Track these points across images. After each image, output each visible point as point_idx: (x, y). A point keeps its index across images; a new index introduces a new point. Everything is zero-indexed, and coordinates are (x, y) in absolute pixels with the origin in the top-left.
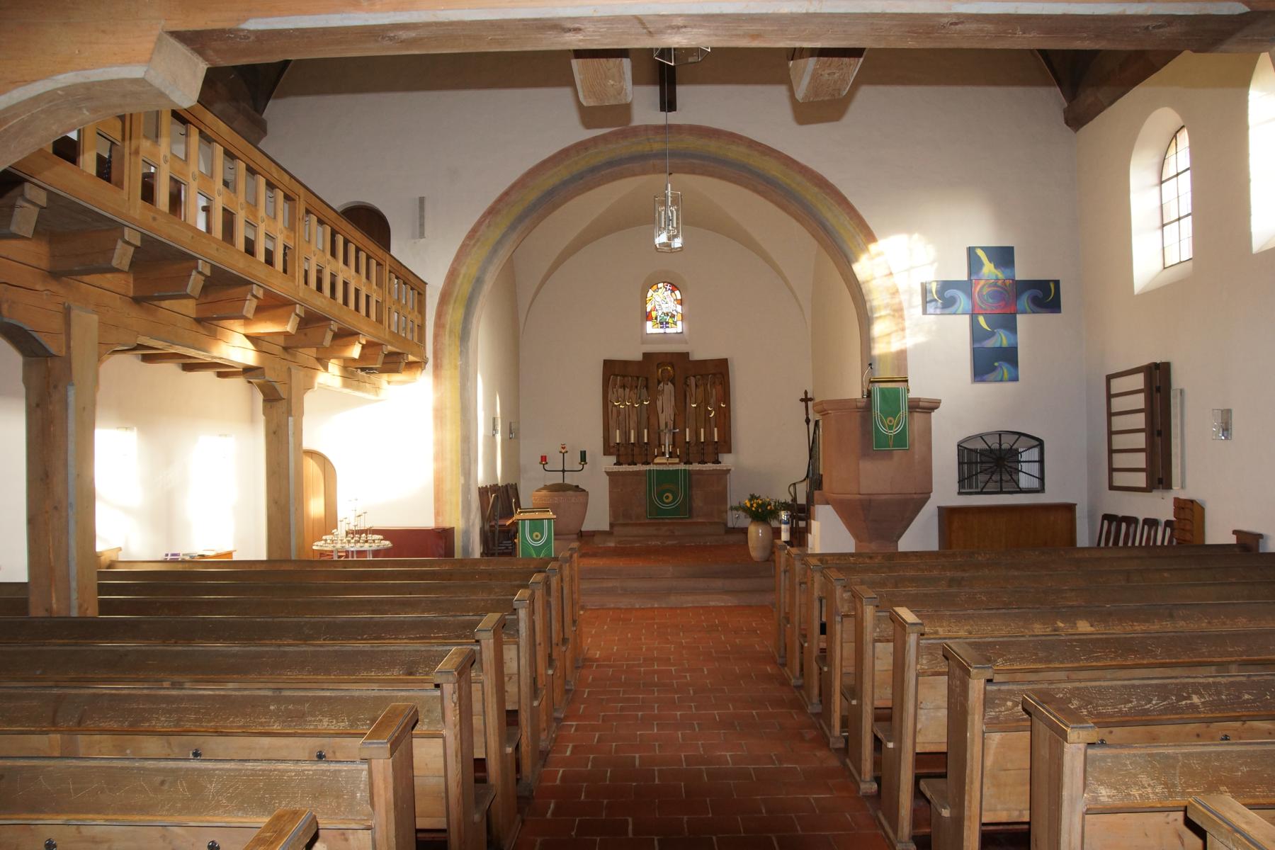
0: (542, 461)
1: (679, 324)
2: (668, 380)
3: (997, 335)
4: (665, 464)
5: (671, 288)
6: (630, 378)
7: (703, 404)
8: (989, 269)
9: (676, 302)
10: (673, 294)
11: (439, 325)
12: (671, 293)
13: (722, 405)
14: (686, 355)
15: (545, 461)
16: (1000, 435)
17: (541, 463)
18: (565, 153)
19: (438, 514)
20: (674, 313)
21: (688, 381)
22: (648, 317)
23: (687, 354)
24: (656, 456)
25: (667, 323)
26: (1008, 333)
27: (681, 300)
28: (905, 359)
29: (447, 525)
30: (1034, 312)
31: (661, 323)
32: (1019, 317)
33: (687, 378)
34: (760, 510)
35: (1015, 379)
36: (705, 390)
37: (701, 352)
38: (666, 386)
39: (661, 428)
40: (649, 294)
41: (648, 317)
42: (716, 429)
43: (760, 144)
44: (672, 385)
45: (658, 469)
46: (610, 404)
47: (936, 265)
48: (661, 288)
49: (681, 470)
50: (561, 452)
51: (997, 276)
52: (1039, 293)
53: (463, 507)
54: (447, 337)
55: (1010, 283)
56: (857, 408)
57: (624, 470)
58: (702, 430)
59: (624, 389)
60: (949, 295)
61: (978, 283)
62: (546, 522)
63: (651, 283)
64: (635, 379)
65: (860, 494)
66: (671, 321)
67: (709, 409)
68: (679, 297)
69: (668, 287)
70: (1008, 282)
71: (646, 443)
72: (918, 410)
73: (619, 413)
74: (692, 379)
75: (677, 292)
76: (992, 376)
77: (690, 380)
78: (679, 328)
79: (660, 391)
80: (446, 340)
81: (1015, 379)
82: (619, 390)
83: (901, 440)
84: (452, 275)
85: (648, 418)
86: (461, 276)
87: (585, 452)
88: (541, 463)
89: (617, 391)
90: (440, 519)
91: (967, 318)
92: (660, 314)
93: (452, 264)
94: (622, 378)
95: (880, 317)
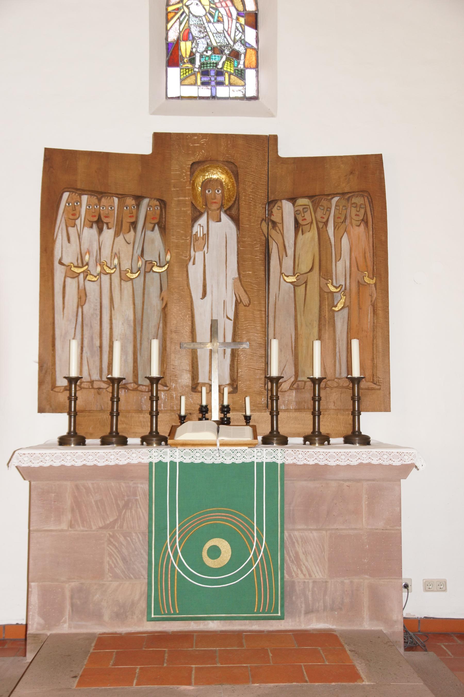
6: (116, 200)
7: (315, 276)
20: (239, 47)
21: (275, 210)
24: (183, 419)
25: (220, 73)
31: (205, 73)
38: (213, 224)
39: (199, 339)
42: (355, 344)
45: (187, 460)
46: (59, 272)
49: (260, 465)
58: (317, 345)
59: (100, 231)
64: (130, 202)
66: (229, 68)
67: (333, 289)
71: (154, 381)
74: (287, 206)
77: (281, 208)
79: (197, 239)
82: (86, 230)
85: (164, 309)
92: (202, 46)
94: (94, 200)
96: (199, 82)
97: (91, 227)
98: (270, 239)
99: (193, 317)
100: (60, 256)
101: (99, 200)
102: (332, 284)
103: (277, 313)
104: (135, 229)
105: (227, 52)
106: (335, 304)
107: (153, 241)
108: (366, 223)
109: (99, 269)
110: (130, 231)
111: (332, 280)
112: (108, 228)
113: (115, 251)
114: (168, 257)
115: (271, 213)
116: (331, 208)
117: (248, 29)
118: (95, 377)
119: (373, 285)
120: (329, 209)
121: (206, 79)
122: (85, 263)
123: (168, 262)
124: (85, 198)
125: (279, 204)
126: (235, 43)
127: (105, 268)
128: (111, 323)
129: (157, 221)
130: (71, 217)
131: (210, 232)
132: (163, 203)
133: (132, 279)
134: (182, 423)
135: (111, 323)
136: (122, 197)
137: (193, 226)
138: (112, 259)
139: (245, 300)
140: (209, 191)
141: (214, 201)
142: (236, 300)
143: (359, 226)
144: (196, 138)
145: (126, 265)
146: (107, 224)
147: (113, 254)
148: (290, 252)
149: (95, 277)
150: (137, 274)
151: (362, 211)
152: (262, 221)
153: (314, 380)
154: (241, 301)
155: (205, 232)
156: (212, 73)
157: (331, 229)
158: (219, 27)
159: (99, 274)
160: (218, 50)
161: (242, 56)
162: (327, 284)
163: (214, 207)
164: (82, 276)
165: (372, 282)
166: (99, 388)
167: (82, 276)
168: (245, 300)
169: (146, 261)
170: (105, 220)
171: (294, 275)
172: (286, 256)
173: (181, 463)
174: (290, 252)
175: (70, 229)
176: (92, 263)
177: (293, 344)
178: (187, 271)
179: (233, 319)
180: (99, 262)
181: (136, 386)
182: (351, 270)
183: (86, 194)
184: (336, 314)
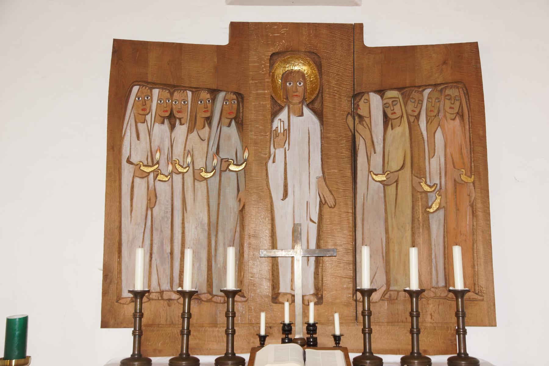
2: (302, 102)
6: (190, 94)
13: (464, 177)
21: (361, 103)
23: (358, 28)
33: (357, 96)
36: (413, 127)
38: (294, 119)
42: (457, 251)
46: (127, 171)
58: (414, 253)
59: (172, 127)
64: (205, 95)
74: (375, 100)
77: (368, 101)
79: (277, 136)
82: (157, 126)
85: (242, 211)
87: (24, 321)
94: (166, 94)
97: (163, 123)
98: (356, 134)
99: (273, 219)
100: (129, 154)
101: (172, 94)
102: (426, 183)
103: (366, 215)
104: (210, 125)
106: (430, 204)
107: (229, 137)
108: (462, 117)
109: (170, 168)
110: (204, 127)
111: (425, 178)
112: (181, 124)
113: (187, 148)
114: (246, 155)
115: (357, 107)
116: (422, 101)
118: (165, 286)
119: (472, 184)
120: (421, 101)
122: (155, 162)
123: (245, 160)
124: (156, 92)
125: (366, 96)
127: (177, 166)
128: (183, 227)
129: (233, 116)
130: (142, 112)
131: (291, 127)
132: (240, 97)
133: (206, 179)
134: (262, 345)
135: (183, 227)
136: (196, 90)
137: (272, 121)
138: (185, 157)
139: (330, 200)
140: (290, 84)
141: (296, 94)
142: (321, 201)
143: (454, 119)
144: (276, 27)
145: (200, 163)
146: (180, 119)
147: (186, 152)
148: (379, 148)
149: (167, 176)
150: (212, 174)
151: (458, 103)
152: (348, 115)
153: (411, 293)
154: (326, 202)
155: (286, 127)
157: (423, 123)
159: (171, 174)
162: (420, 183)
163: (296, 100)
164: (152, 176)
165: (471, 180)
166: (170, 300)
167: (152, 176)
168: (330, 200)
169: (222, 159)
170: (178, 115)
171: (384, 173)
172: (375, 153)
174: (379, 148)
175: (140, 125)
176: (163, 162)
177: (384, 249)
178: (267, 170)
179: (317, 222)
180: (170, 160)
181: (211, 297)
182: (446, 168)
183: (157, 88)
184: (431, 216)
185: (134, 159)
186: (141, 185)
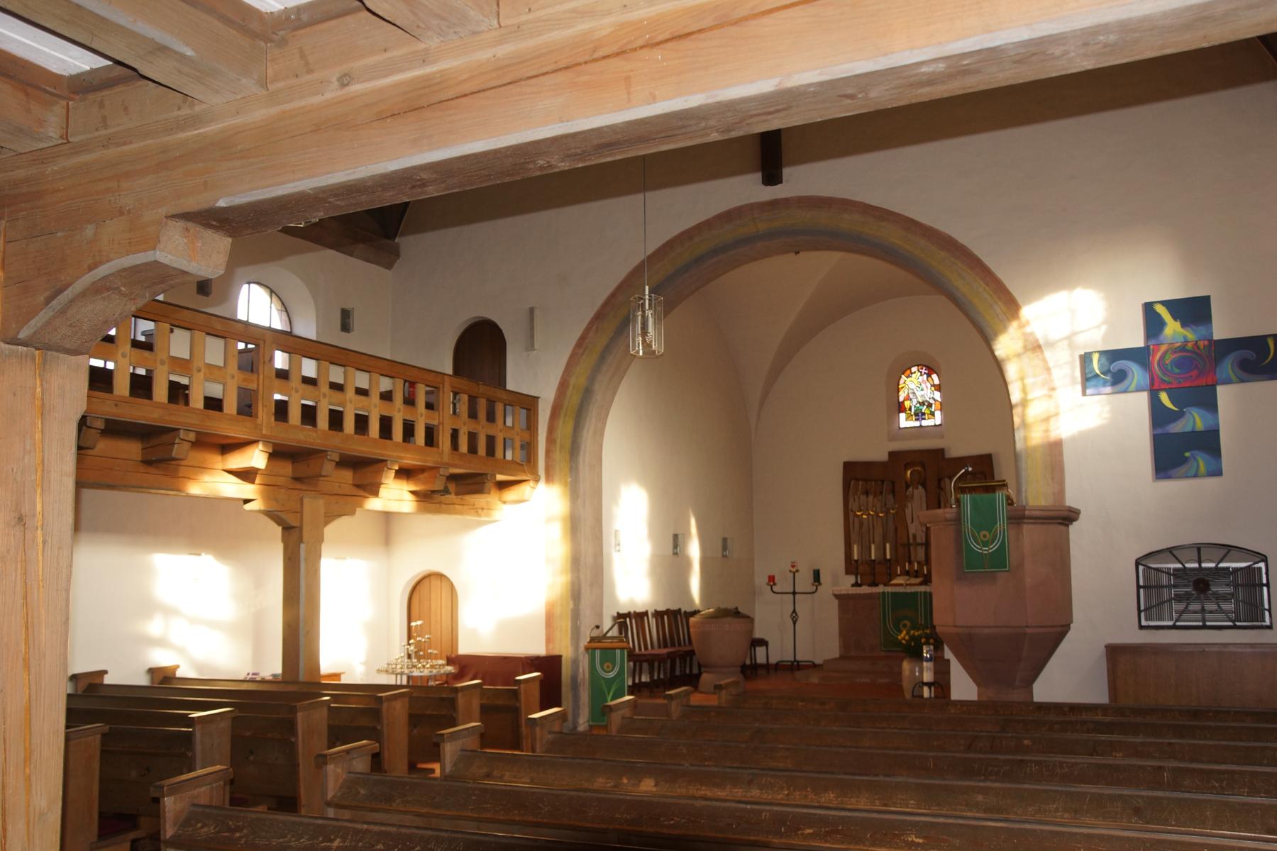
0: (769, 581)
1: (938, 414)
3: (1188, 415)
4: (902, 585)
5: (926, 372)
6: (873, 483)
8: (1173, 329)
9: (933, 389)
10: (930, 379)
11: (550, 440)
12: (927, 377)
14: (941, 452)
15: (774, 581)
16: (1199, 549)
17: (768, 584)
18: (669, 246)
19: (549, 640)
20: (932, 401)
22: (901, 408)
25: (924, 414)
26: (1203, 412)
27: (939, 385)
28: (1061, 454)
29: (556, 652)
30: (1242, 381)
31: (916, 414)
32: (1220, 389)
33: (940, 480)
34: (913, 644)
35: (1218, 472)
37: (958, 448)
38: (915, 491)
40: (902, 381)
41: (901, 408)
43: (876, 208)
44: (923, 491)
46: (851, 513)
47: (1104, 328)
48: (915, 373)
49: (921, 592)
50: (790, 571)
51: (1185, 337)
52: (1250, 354)
53: (572, 634)
54: (558, 452)
55: (1204, 346)
56: (947, 520)
57: (862, 592)
59: (867, 496)
60: (1116, 369)
61: (1158, 350)
62: (618, 652)
63: (906, 370)
64: (879, 483)
65: (955, 626)
68: (937, 382)
69: (923, 371)
70: (1201, 344)
72: (1026, 521)
73: (861, 524)
75: (935, 376)
76: (1182, 470)
78: (938, 419)
80: (557, 455)
81: (1218, 472)
83: (998, 559)
84: (563, 386)
85: (896, 529)
86: (571, 388)
88: (768, 584)
89: (859, 498)
90: (551, 646)
91: (1142, 399)
92: (915, 401)
93: (563, 375)
95: (1035, 399)
96: (914, 419)
105: (926, 404)
114: (896, 506)
117: (935, 392)
121: (917, 417)
126: (930, 398)
132: (893, 483)
145: (878, 510)
156: (920, 414)
158: (922, 393)
160: (922, 404)
161: (933, 405)
173: (892, 593)
185: (854, 510)
186: (857, 520)
